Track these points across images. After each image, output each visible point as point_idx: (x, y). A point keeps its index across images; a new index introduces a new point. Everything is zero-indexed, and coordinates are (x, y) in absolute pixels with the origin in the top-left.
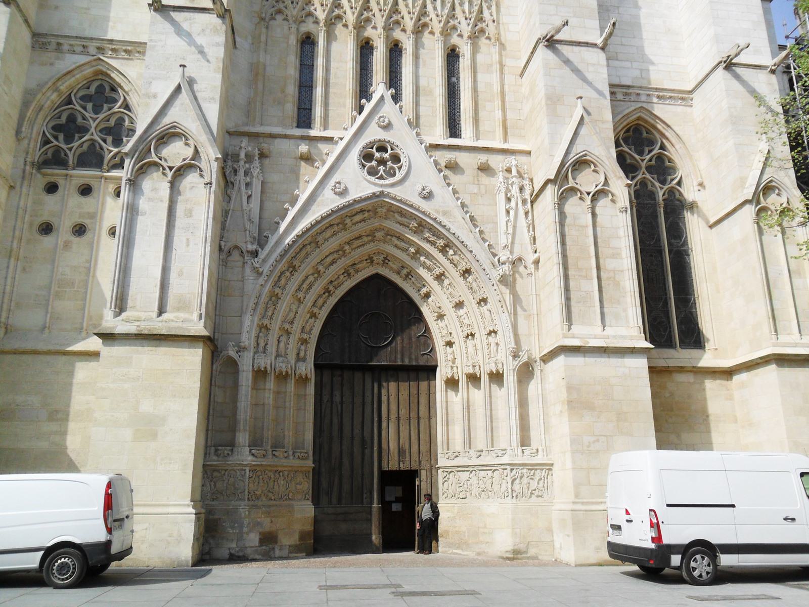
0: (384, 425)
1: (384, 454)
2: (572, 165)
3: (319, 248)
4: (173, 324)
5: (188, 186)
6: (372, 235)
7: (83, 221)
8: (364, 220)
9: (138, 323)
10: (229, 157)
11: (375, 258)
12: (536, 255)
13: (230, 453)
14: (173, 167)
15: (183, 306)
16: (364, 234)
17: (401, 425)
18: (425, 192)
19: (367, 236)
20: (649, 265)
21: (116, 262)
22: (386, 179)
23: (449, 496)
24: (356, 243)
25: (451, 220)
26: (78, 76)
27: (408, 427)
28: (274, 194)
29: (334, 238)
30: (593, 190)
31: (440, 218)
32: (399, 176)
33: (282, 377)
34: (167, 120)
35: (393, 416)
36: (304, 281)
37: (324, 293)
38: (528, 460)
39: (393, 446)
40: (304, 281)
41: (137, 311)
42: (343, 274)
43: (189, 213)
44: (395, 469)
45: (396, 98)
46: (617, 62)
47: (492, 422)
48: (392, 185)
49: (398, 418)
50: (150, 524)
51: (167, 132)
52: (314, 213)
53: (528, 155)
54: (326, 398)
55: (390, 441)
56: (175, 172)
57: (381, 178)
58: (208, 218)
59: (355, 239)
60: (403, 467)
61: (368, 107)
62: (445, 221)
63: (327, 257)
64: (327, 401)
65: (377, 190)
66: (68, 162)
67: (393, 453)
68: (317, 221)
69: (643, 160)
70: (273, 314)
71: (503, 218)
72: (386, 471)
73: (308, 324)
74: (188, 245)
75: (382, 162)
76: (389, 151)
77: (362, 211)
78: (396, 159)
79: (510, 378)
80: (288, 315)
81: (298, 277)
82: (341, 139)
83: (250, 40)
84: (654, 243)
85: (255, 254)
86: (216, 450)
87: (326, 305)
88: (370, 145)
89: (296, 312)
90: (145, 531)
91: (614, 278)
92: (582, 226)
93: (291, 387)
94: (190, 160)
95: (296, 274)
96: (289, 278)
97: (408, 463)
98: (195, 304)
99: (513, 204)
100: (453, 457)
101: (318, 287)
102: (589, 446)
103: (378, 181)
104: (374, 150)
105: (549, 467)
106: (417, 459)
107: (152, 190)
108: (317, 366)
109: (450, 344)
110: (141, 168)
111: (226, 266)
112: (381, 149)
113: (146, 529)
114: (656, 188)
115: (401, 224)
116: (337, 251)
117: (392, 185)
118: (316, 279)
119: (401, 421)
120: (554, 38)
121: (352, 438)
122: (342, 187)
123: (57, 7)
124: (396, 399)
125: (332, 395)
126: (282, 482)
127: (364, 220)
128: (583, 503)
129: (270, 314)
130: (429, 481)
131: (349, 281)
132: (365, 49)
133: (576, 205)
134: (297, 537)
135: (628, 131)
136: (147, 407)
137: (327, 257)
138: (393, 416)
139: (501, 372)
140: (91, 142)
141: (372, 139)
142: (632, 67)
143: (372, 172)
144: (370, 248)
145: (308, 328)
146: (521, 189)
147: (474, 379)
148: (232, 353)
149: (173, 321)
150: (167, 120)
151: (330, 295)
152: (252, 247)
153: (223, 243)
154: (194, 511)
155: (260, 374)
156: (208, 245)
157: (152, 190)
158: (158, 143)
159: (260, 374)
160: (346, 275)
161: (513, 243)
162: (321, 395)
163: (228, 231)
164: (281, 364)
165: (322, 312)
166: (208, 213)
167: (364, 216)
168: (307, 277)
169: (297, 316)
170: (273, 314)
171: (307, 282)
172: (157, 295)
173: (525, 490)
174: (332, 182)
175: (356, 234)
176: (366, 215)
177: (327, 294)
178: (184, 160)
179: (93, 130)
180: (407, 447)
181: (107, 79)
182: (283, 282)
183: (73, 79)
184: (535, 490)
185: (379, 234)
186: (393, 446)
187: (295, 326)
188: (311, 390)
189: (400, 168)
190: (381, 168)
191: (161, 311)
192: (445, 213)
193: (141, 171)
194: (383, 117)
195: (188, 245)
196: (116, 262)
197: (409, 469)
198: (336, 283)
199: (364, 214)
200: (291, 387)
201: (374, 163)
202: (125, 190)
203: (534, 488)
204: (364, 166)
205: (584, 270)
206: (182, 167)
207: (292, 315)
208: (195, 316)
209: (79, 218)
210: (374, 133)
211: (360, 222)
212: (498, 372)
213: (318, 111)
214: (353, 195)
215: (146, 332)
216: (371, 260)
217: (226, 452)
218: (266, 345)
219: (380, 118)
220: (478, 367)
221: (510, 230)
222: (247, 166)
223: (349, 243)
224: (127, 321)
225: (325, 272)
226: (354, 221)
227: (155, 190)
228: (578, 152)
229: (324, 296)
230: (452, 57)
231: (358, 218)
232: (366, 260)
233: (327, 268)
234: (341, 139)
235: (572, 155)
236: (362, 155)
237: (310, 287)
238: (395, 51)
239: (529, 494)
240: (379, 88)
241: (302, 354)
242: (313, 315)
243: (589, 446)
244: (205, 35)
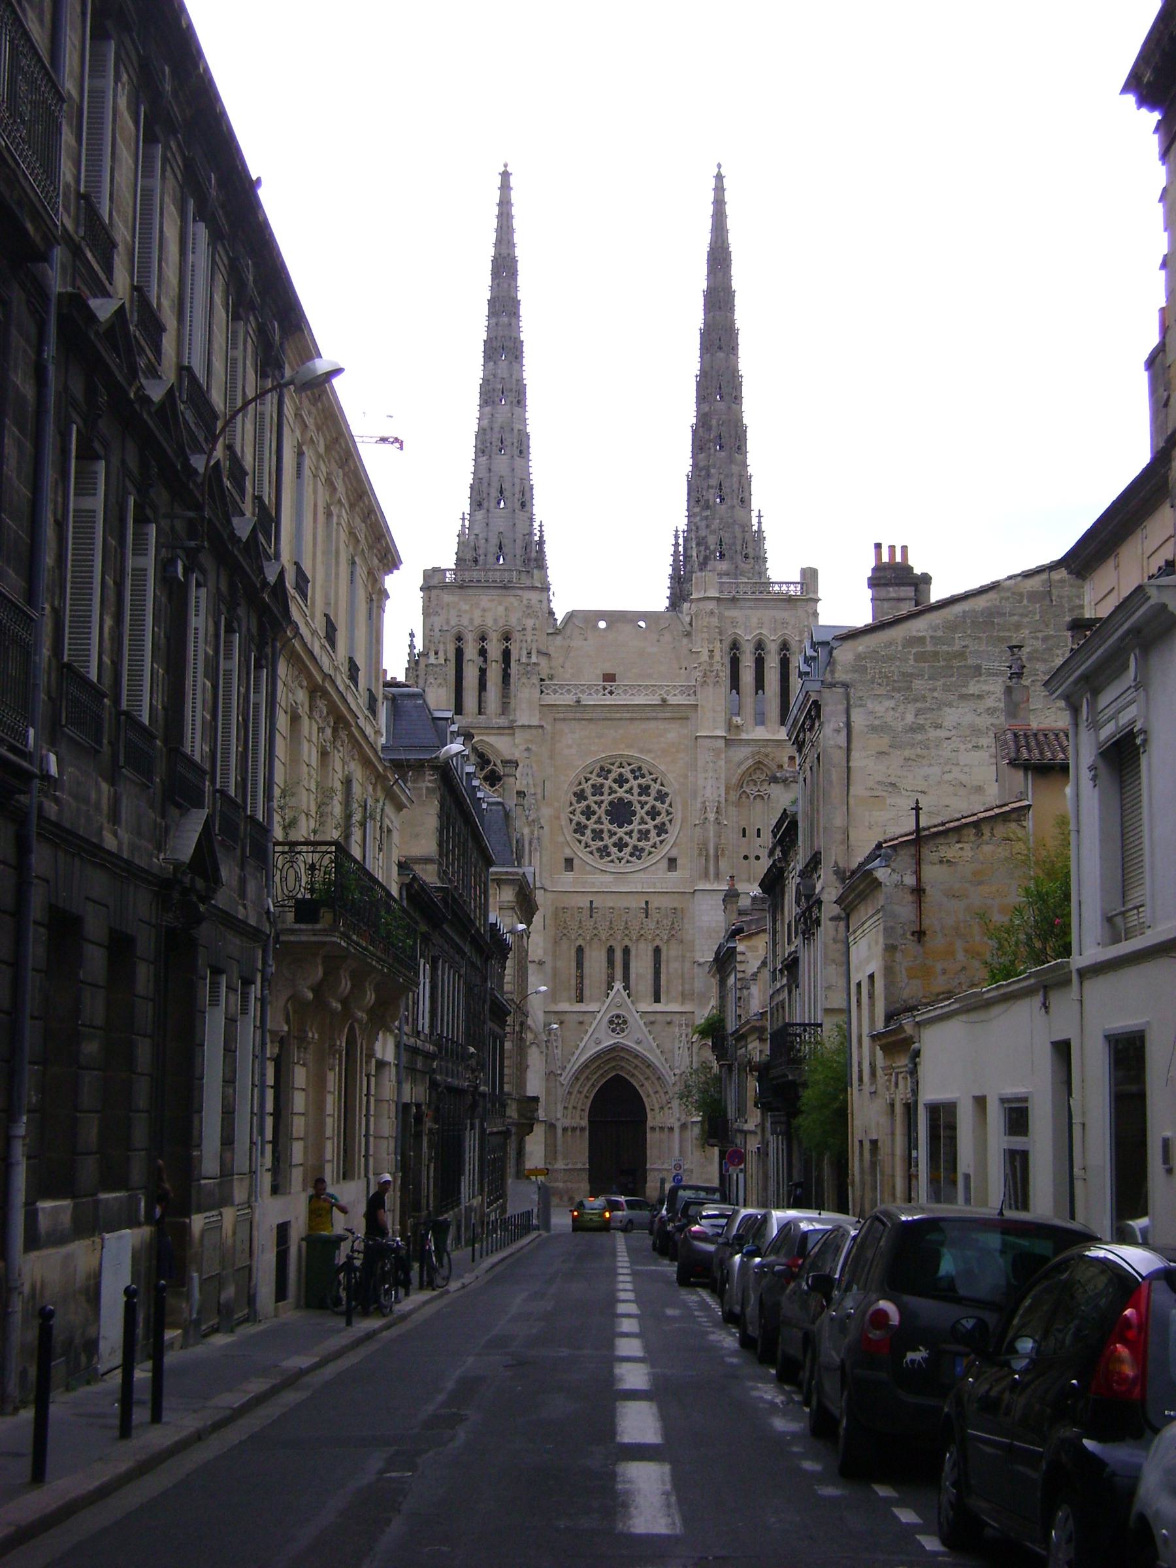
6: (613, 1059)
32: (625, 1033)
33: (574, 1129)
45: (626, 988)
61: (612, 994)
65: (616, 1041)
75: (618, 1024)
78: (625, 1022)
79: (677, 1130)
85: (561, 1075)
93: (578, 1133)
109: (652, 1110)
112: (618, 1016)
132: (611, 951)
144: (613, 1064)
146: (687, 1035)
147: (662, 1128)
152: (559, 1072)
155: (565, 1130)
159: (565, 1130)
200: (578, 1133)
230: (657, 951)
238: (626, 951)
240: (618, 985)
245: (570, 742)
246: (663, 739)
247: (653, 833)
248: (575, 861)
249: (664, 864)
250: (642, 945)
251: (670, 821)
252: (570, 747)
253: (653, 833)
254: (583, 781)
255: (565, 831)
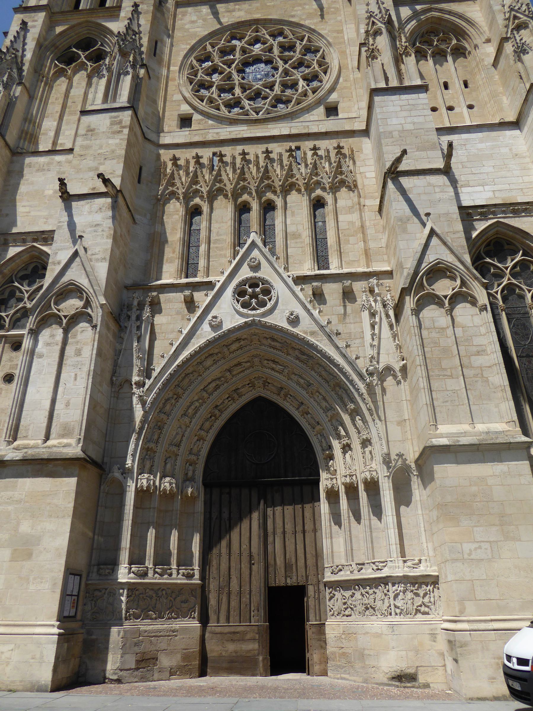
0: (270, 539)
1: (271, 569)
2: (426, 274)
3: (201, 376)
4: (55, 449)
5: (80, 330)
7: (13, 371)
8: (241, 348)
9: (25, 450)
10: (126, 307)
11: (256, 382)
12: (405, 362)
13: (111, 571)
14: (68, 316)
15: (66, 433)
16: (244, 361)
17: (287, 540)
18: (292, 317)
19: (246, 362)
20: (527, 364)
21: (14, 398)
22: (258, 309)
23: (336, 613)
24: (236, 371)
25: (318, 339)
26: (17, 261)
27: (294, 541)
28: (162, 333)
29: (215, 366)
30: (450, 293)
31: (309, 338)
32: (269, 306)
34: (65, 279)
35: (279, 531)
36: (189, 407)
37: (211, 417)
38: (410, 572)
39: (280, 561)
40: (189, 407)
41: (29, 440)
42: (227, 398)
43: (78, 353)
44: (282, 584)
46: (470, 188)
47: (371, 532)
48: (264, 315)
49: (284, 533)
50: (15, 645)
51: (65, 289)
52: (194, 345)
53: (390, 276)
54: (215, 515)
55: (277, 555)
56: (69, 320)
57: (254, 309)
58: (92, 354)
59: (234, 366)
60: (289, 582)
62: (313, 340)
63: (210, 383)
64: (216, 518)
66: (5, 326)
67: (280, 568)
68: (195, 352)
69: (507, 268)
70: (159, 438)
71: (368, 332)
72: (273, 587)
73: (196, 446)
74: (76, 379)
75: (254, 296)
76: (261, 286)
77: (238, 340)
78: (267, 292)
80: (175, 438)
81: (183, 403)
82: (219, 281)
83: (148, 216)
84: (529, 343)
86: (98, 570)
87: (213, 428)
88: (243, 283)
89: (183, 436)
90: (11, 652)
91: (482, 374)
92: (442, 328)
94: (82, 308)
95: (181, 401)
96: (175, 405)
97: (295, 578)
98: (77, 431)
99: (377, 319)
100: (336, 571)
101: (204, 412)
102: (470, 554)
103: (250, 312)
104: (247, 287)
105: (434, 581)
106: (304, 574)
107: (50, 337)
108: (208, 485)
110: (42, 319)
111: (117, 398)
112: (254, 285)
113: (12, 650)
114: (524, 291)
115: (274, 348)
116: (219, 379)
117: (264, 315)
118: (201, 405)
119: (287, 535)
120: (398, 170)
121: (240, 554)
122: (219, 320)
123: (7, 215)
124: (282, 514)
125: (220, 513)
126: (165, 601)
127: (241, 348)
128: (468, 621)
129: (156, 437)
130: (316, 596)
131: (234, 405)
133: (434, 310)
134: (179, 656)
135: (488, 245)
136: (25, 527)
137: (210, 383)
138: (279, 531)
139: (376, 480)
140: (23, 310)
141: (244, 277)
142: (484, 191)
143: (245, 305)
145: (195, 450)
148: (117, 474)
149: (55, 446)
150: (65, 279)
151: (216, 419)
153: (114, 379)
154: (56, 631)
156: (91, 377)
157: (50, 337)
158: (59, 298)
160: (230, 399)
161: (378, 354)
162: (210, 513)
163: (120, 367)
164: (166, 484)
165: (209, 435)
166: (93, 350)
167: (240, 344)
168: (192, 403)
169: (184, 439)
170: (159, 438)
171: (193, 407)
172: (45, 425)
173: (410, 606)
174: (209, 317)
175: (235, 362)
176: (242, 343)
177: (213, 418)
178: (77, 309)
179: (26, 299)
180: (293, 560)
181: (40, 261)
182: (168, 407)
183: (14, 264)
184: (421, 606)
185: (256, 359)
186: (280, 561)
187: (182, 448)
188: (200, 506)
189: (270, 300)
190: (254, 301)
191: (47, 437)
192: (313, 333)
193: (41, 323)
194: (253, 258)
195: (76, 379)
196: (14, 398)
197: (296, 584)
198: (221, 406)
199: (240, 342)
201: (247, 297)
202: (27, 338)
203: (419, 604)
204: (238, 301)
205: (449, 370)
206: (74, 315)
207: (179, 438)
208: (72, 441)
209: (10, 368)
210: (245, 273)
211: (238, 350)
212: (372, 478)
213: (202, 263)
214: (227, 326)
215: (30, 458)
216: (251, 384)
217: (107, 571)
218: (152, 466)
219: (251, 259)
220: (354, 477)
221: (375, 343)
222: (139, 312)
223: (229, 370)
224: (17, 449)
225: (209, 398)
226: (231, 350)
227: (52, 336)
228: (431, 261)
229: (211, 420)
231: (234, 347)
232: (248, 384)
233: (210, 394)
234: (219, 281)
235: (424, 265)
236: (237, 291)
237: (197, 410)
239: (414, 611)
241: (190, 474)
242: (201, 439)
243: (470, 554)
244: (101, 212)
245: (194, 18)
246: (307, 7)
247: (301, 83)
248: (196, 117)
249: (321, 110)
250: (293, 197)
251: (325, 73)
252: (193, 22)
253: (301, 83)
254: (209, 48)
255: (184, 90)
